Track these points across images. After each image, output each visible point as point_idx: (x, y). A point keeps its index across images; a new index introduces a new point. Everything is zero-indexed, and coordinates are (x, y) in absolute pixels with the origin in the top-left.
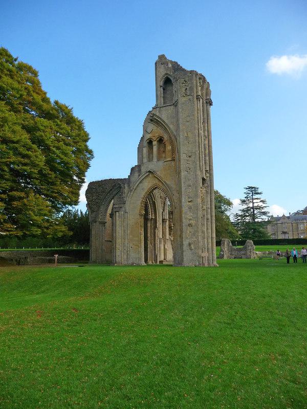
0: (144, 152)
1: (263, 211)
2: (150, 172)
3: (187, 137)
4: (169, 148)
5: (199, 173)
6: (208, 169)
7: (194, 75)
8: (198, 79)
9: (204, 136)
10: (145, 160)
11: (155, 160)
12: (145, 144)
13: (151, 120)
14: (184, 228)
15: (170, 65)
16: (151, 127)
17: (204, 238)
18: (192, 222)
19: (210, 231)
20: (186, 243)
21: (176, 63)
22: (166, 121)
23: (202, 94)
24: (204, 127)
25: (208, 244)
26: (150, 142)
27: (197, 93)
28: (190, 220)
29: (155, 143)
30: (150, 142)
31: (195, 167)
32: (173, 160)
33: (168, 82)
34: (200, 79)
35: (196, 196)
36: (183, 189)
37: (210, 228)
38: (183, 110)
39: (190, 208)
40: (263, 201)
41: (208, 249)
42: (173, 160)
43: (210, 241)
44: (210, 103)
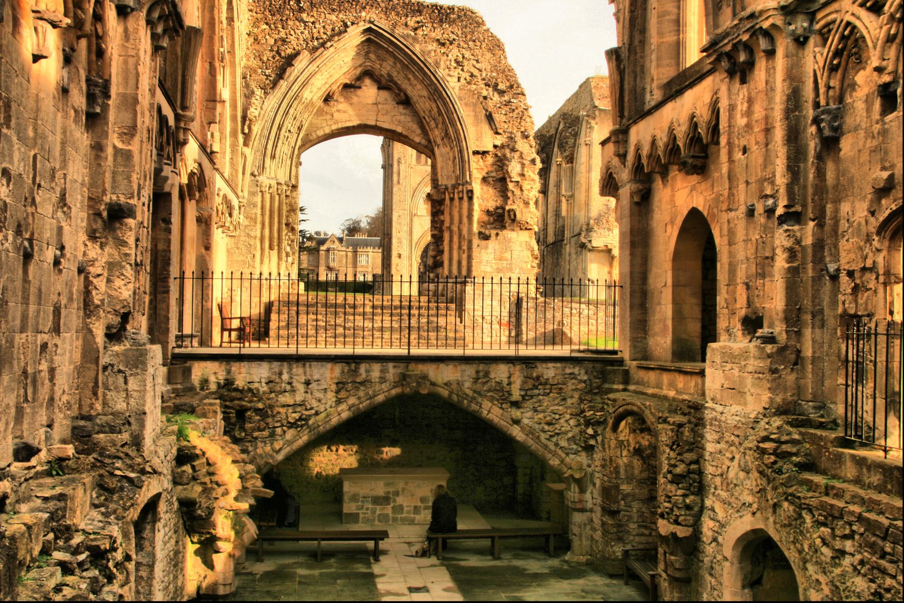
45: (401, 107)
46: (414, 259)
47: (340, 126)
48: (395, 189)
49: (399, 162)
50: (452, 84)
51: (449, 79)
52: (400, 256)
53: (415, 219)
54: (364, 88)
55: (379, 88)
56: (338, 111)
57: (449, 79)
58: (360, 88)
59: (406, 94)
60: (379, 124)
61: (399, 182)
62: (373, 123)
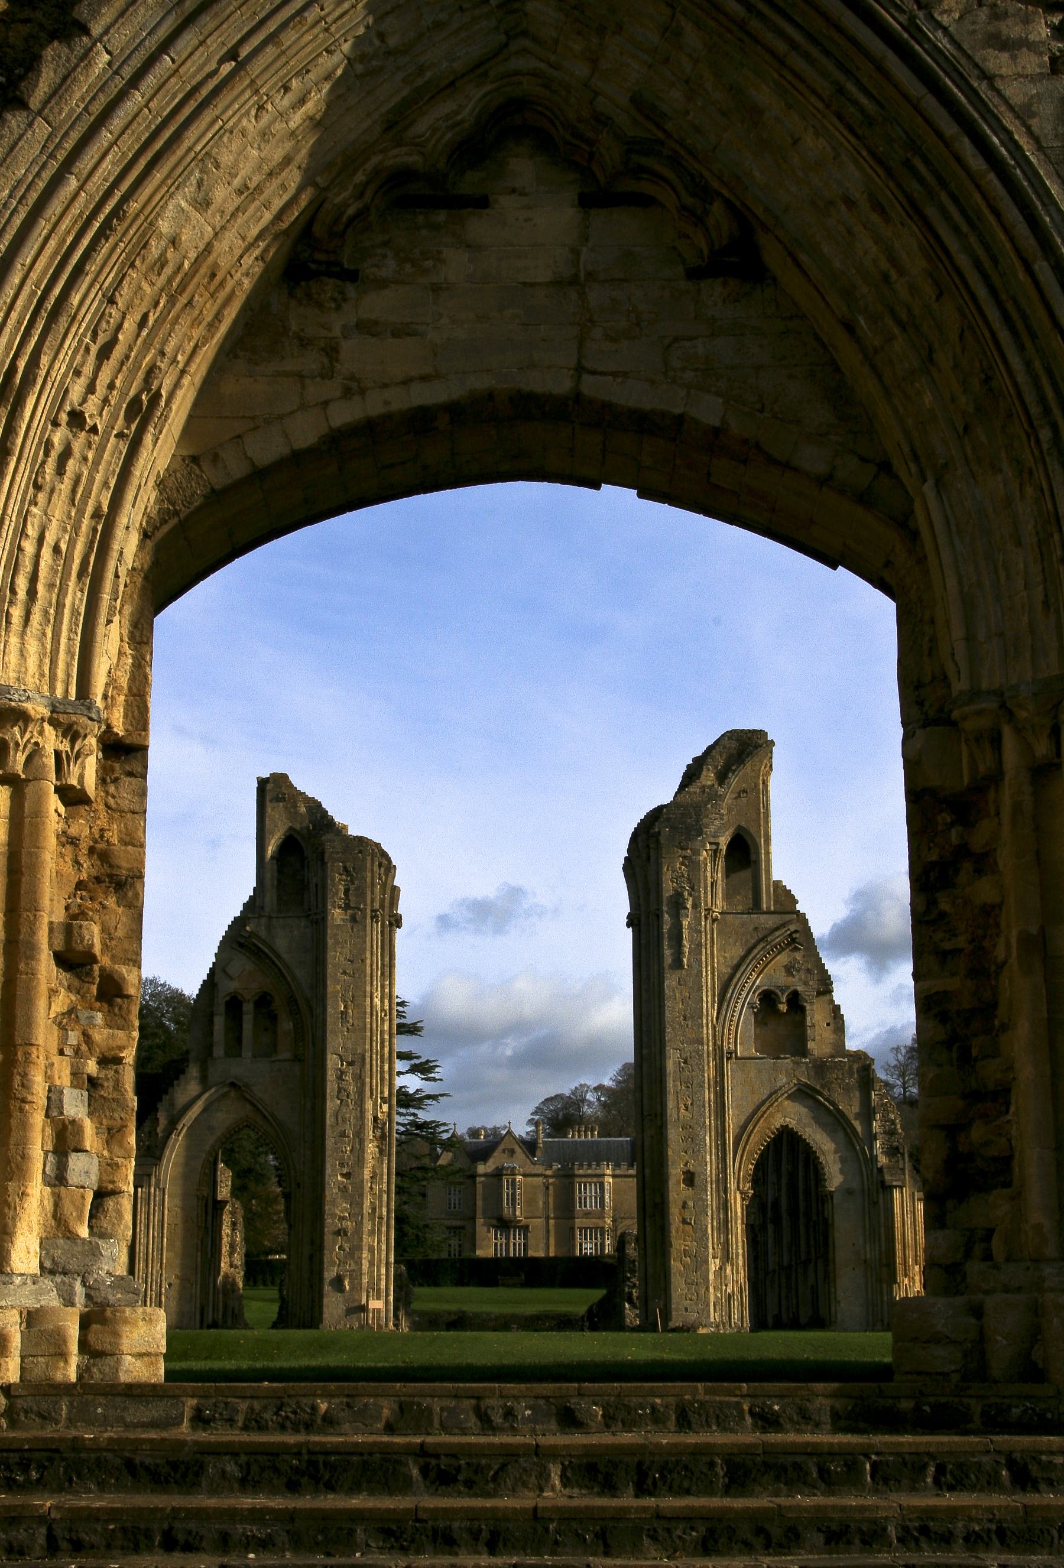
0: (216, 1027)
1: (423, 1116)
2: (233, 1085)
3: (344, 1014)
4: (286, 1025)
5: (369, 1105)
6: (386, 1094)
7: (369, 858)
8: (376, 868)
9: (383, 1010)
10: (219, 1051)
11: (247, 1053)
12: (220, 1008)
13: (241, 945)
14: (328, 1238)
15: (303, 810)
16: (241, 964)
17: (371, 1263)
18: (349, 1225)
19: (384, 1247)
20: (330, 1274)
21: (319, 805)
22: (285, 956)
23: (382, 906)
24: (383, 987)
25: (379, 1279)
26: (234, 1005)
27: (372, 906)
28: (344, 1218)
29: (248, 1008)
30: (234, 1005)
31: (361, 1093)
32: (297, 1059)
33: (290, 845)
34: (380, 865)
35: (360, 1161)
36: (330, 1142)
37: (384, 1238)
38: (337, 943)
39: (344, 1190)
40: (423, 1069)
41: (379, 1290)
42: (297, 1059)
43: (383, 1271)
44: (397, 922)
45: (714, 291)
46: (732, 1185)
47: (374, 406)
48: (670, 982)
49: (677, 904)
50: (1016, 92)
51: (998, 62)
52: (690, 1179)
53: (729, 1067)
54: (506, 203)
55: (587, 202)
56: (367, 328)
57: (998, 62)
58: (482, 203)
59: (739, 214)
60: (591, 387)
61: (678, 964)
62: (560, 385)
